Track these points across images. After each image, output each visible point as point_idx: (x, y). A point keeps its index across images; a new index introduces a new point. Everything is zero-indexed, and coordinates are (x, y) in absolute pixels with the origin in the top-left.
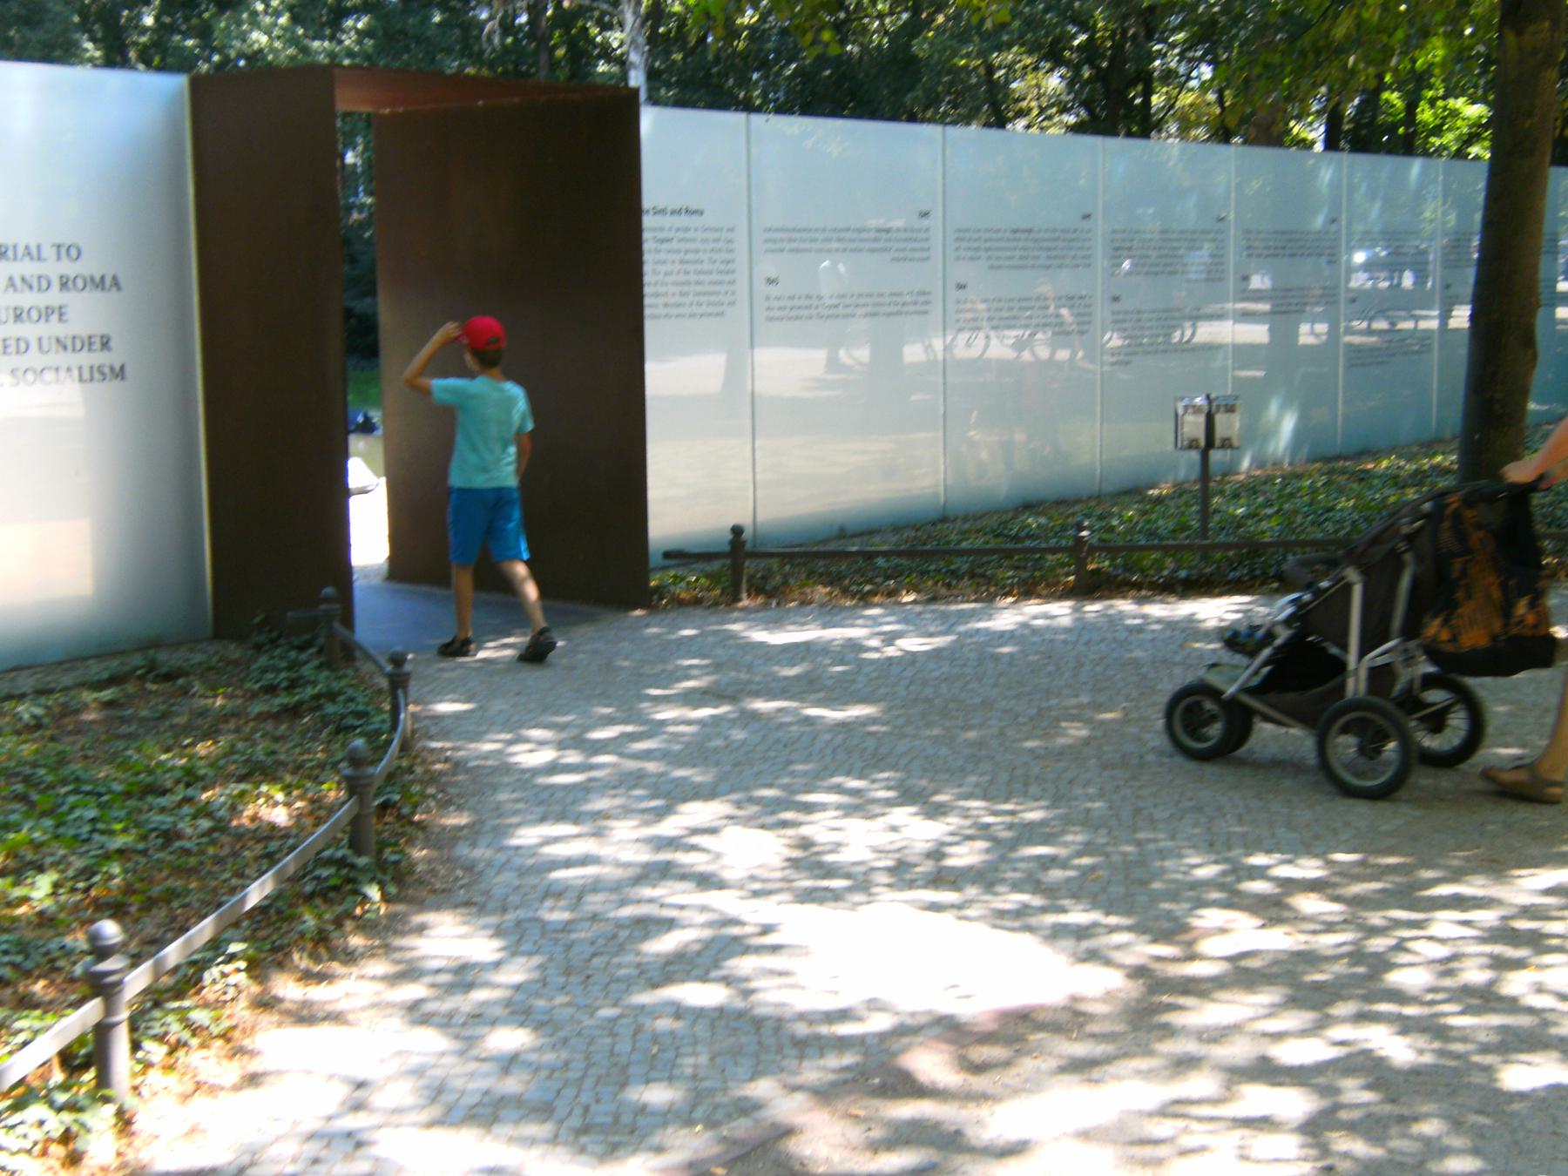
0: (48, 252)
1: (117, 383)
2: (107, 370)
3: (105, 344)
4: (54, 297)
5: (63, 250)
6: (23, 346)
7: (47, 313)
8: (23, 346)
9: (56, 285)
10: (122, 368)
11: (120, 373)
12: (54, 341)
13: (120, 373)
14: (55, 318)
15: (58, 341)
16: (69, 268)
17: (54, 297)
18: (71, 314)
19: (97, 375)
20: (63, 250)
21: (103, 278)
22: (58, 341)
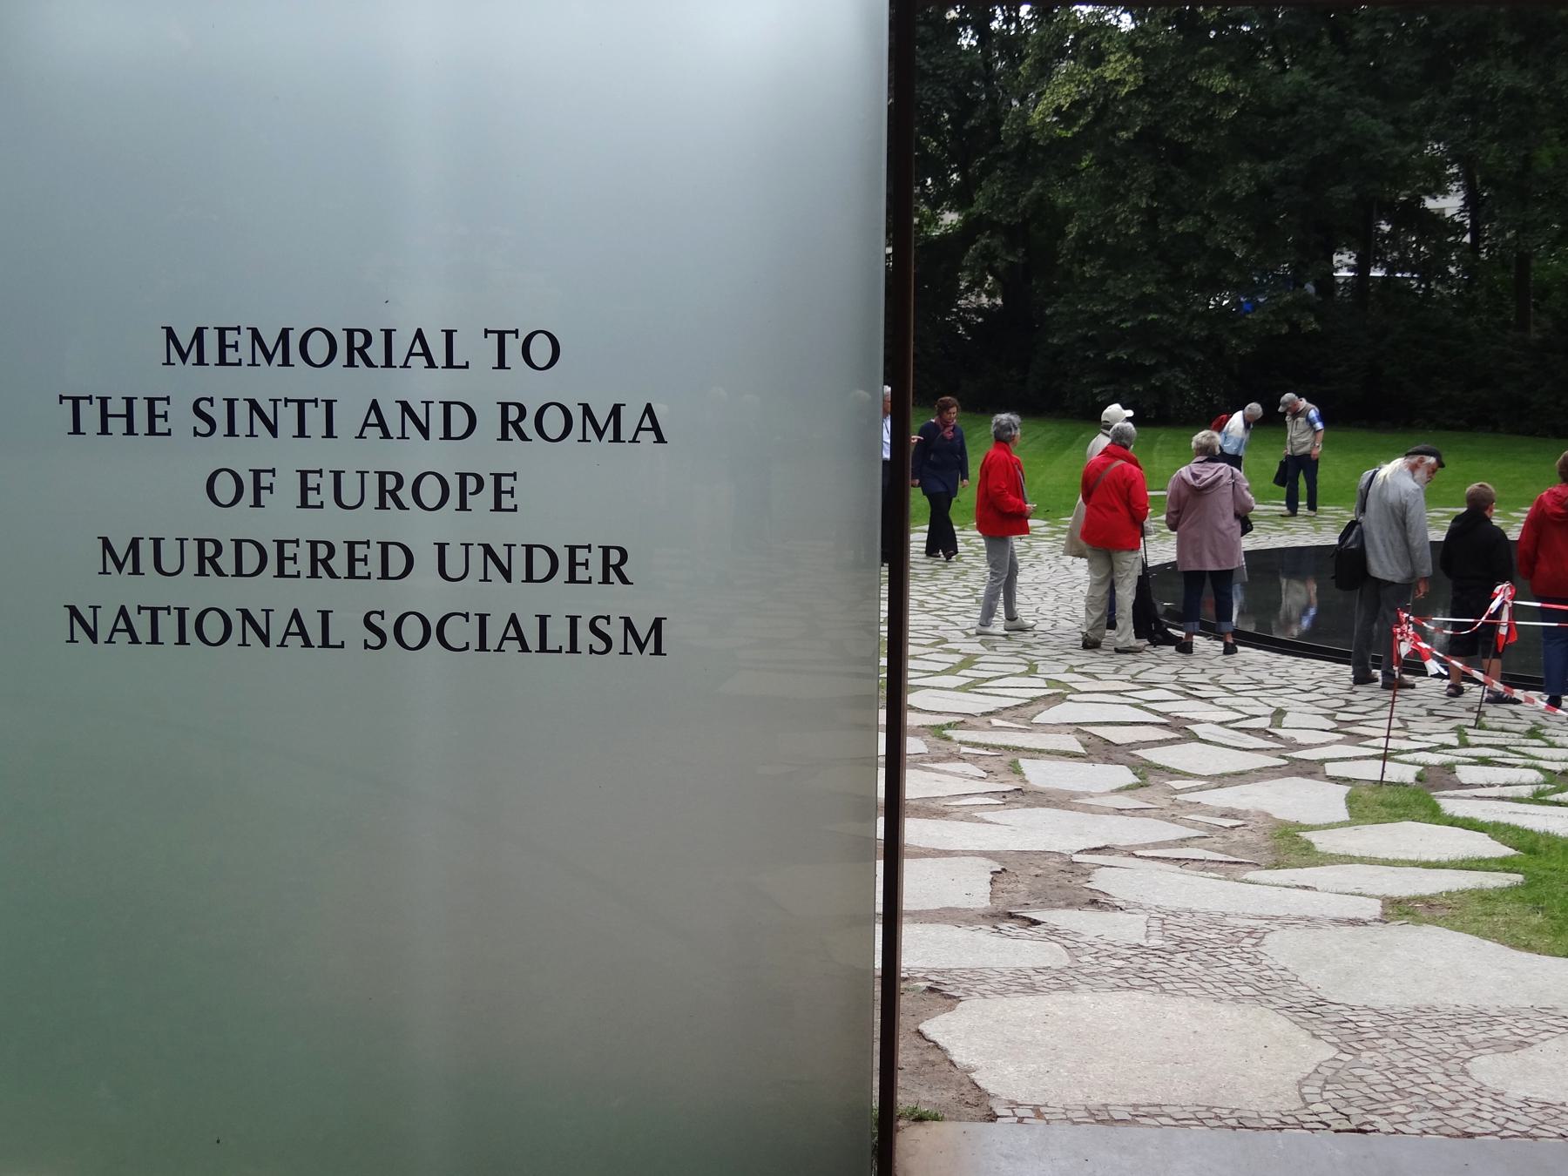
0: (475, 349)
2: (615, 631)
5: (513, 346)
6: (397, 561)
7: (462, 490)
8: (397, 561)
9: (489, 421)
10: (657, 625)
12: (477, 554)
18: (524, 492)
19: (585, 636)
20: (513, 346)
21: (616, 411)
22: (488, 550)
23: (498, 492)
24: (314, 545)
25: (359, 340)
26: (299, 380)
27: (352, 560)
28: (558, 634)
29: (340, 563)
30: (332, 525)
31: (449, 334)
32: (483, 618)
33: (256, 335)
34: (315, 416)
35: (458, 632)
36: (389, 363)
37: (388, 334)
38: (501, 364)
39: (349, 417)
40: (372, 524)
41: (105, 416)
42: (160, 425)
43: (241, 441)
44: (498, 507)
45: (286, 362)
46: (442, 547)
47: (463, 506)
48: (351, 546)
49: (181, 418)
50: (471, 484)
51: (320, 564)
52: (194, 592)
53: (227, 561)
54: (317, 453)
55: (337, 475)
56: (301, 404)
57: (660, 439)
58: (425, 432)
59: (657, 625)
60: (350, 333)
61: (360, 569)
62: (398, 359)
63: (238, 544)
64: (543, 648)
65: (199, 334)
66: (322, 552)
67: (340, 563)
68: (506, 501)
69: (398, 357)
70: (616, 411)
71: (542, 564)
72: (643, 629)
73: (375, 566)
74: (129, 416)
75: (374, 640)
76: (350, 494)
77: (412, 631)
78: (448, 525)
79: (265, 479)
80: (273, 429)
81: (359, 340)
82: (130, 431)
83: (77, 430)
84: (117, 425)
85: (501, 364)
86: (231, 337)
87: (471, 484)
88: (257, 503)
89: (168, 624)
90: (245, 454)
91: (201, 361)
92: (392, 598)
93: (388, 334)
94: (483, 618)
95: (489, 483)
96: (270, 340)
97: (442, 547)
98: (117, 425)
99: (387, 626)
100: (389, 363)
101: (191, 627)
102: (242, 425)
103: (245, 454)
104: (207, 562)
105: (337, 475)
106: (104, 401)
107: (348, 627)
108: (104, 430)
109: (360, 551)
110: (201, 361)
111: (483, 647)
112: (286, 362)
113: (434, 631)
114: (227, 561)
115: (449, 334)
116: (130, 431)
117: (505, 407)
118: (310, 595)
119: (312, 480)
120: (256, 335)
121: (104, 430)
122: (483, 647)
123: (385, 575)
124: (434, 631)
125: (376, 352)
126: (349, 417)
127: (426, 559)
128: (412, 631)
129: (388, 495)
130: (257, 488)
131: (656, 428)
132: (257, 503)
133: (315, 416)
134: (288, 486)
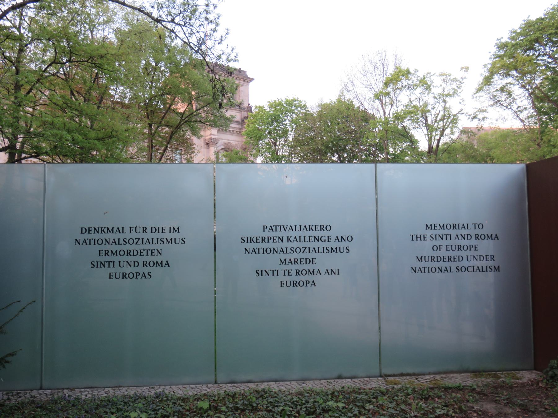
0: (471, 226)
1: (497, 272)
3: (492, 258)
4: (473, 242)
5: (477, 226)
6: (461, 259)
7: (470, 247)
8: (461, 259)
10: (499, 267)
11: (497, 269)
12: (472, 257)
13: (497, 269)
14: (473, 249)
15: (474, 256)
16: (479, 232)
17: (473, 242)
18: (478, 247)
19: (489, 269)
20: (477, 226)
21: (492, 235)
23: (475, 248)
24: (448, 256)
25: (454, 225)
26: (446, 232)
27: (454, 259)
28: (484, 269)
29: (452, 259)
30: (451, 253)
31: (468, 224)
32: (473, 267)
33: (439, 225)
34: (448, 237)
35: (470, 269)
36: (459, 229)
37: (459, 224)
38: (475, 229)
39: (453, 237)
40: (457, 253)
41: (417, 237)
42: (425, 239)
43: (438, 241)
44: (475, 250)
45: (444, 229)
46: (467, 256)
47: (470, 250)
48: (454, 256)
49: (428, 237)
50: (471, 246)
51: (449, 259)
52: (430, 264)
53: (435, 259)
54: (449, 242)
55: (452, 246)
56: (446, 235)
57: (498, 239)
58: (464, 239)
59: (499, 267)
60: (453, 224)
61: (455, 260)
62: (460, 228)
63: (437, 257)
64: (482, 271)
65: (431, 225)
66: (450, 258)
67: (452, 259)
68: (476, 249)
69: (460, 228)
70: (492, 235)
71: (482, 258)
72: (497, 268)
73: (457, 259)
74: (421, 238)
75: (458, 271)
76: (454, 249)
77: (463, 269)
78: (468, 253)
79: (441, 247)
80: (442, 239)
81: (454, 225)
82: (421, 240)
83: (413, 240)
84: (419, 239)
85: (475, 229)
86: (436, 225)
87: (471, 246)
88: (440, 250)
89: (427, 270)
90: (438, 243)
91: (431, 229)
92: (460, 264)
93: (459, 224)
94: (473, 267)
95: (474, 246)
96: (442, 226)
97: (467, 256)
98: (419, 239)
99: (460, 269)
100: (459, 229)
101: (430, 270)
102: (437, 238)
103: (438, 243)
104: (433, 260)
105: (452, 246)
106: (417, 235)
107: (454, 269)
108: (417, 240)
109: (455, 257)
110: (431, 229)
111: (474, 271)
112: (444, 229)
113: (467, 269)
114: (435, 259)
115: (468, 224)
116: (421, 240)
117: (476, 235)
118: (447, 264)
119: (448, 247)
120: (439, 225)
121: (417, 240)
122: (474, 271)
123: (459, 261)
124: (467, 269)
125: (457, 227)
126: (453, 237)
127: (465, 258)
128: (463, 269)
129: (459, 249)
130: (440, 248)
131: (497, 237)
132: (440, 250)
133: (448, 237)
134: (444, 248)
